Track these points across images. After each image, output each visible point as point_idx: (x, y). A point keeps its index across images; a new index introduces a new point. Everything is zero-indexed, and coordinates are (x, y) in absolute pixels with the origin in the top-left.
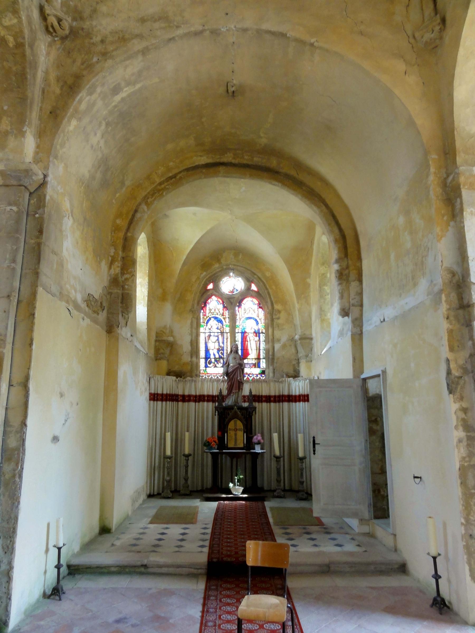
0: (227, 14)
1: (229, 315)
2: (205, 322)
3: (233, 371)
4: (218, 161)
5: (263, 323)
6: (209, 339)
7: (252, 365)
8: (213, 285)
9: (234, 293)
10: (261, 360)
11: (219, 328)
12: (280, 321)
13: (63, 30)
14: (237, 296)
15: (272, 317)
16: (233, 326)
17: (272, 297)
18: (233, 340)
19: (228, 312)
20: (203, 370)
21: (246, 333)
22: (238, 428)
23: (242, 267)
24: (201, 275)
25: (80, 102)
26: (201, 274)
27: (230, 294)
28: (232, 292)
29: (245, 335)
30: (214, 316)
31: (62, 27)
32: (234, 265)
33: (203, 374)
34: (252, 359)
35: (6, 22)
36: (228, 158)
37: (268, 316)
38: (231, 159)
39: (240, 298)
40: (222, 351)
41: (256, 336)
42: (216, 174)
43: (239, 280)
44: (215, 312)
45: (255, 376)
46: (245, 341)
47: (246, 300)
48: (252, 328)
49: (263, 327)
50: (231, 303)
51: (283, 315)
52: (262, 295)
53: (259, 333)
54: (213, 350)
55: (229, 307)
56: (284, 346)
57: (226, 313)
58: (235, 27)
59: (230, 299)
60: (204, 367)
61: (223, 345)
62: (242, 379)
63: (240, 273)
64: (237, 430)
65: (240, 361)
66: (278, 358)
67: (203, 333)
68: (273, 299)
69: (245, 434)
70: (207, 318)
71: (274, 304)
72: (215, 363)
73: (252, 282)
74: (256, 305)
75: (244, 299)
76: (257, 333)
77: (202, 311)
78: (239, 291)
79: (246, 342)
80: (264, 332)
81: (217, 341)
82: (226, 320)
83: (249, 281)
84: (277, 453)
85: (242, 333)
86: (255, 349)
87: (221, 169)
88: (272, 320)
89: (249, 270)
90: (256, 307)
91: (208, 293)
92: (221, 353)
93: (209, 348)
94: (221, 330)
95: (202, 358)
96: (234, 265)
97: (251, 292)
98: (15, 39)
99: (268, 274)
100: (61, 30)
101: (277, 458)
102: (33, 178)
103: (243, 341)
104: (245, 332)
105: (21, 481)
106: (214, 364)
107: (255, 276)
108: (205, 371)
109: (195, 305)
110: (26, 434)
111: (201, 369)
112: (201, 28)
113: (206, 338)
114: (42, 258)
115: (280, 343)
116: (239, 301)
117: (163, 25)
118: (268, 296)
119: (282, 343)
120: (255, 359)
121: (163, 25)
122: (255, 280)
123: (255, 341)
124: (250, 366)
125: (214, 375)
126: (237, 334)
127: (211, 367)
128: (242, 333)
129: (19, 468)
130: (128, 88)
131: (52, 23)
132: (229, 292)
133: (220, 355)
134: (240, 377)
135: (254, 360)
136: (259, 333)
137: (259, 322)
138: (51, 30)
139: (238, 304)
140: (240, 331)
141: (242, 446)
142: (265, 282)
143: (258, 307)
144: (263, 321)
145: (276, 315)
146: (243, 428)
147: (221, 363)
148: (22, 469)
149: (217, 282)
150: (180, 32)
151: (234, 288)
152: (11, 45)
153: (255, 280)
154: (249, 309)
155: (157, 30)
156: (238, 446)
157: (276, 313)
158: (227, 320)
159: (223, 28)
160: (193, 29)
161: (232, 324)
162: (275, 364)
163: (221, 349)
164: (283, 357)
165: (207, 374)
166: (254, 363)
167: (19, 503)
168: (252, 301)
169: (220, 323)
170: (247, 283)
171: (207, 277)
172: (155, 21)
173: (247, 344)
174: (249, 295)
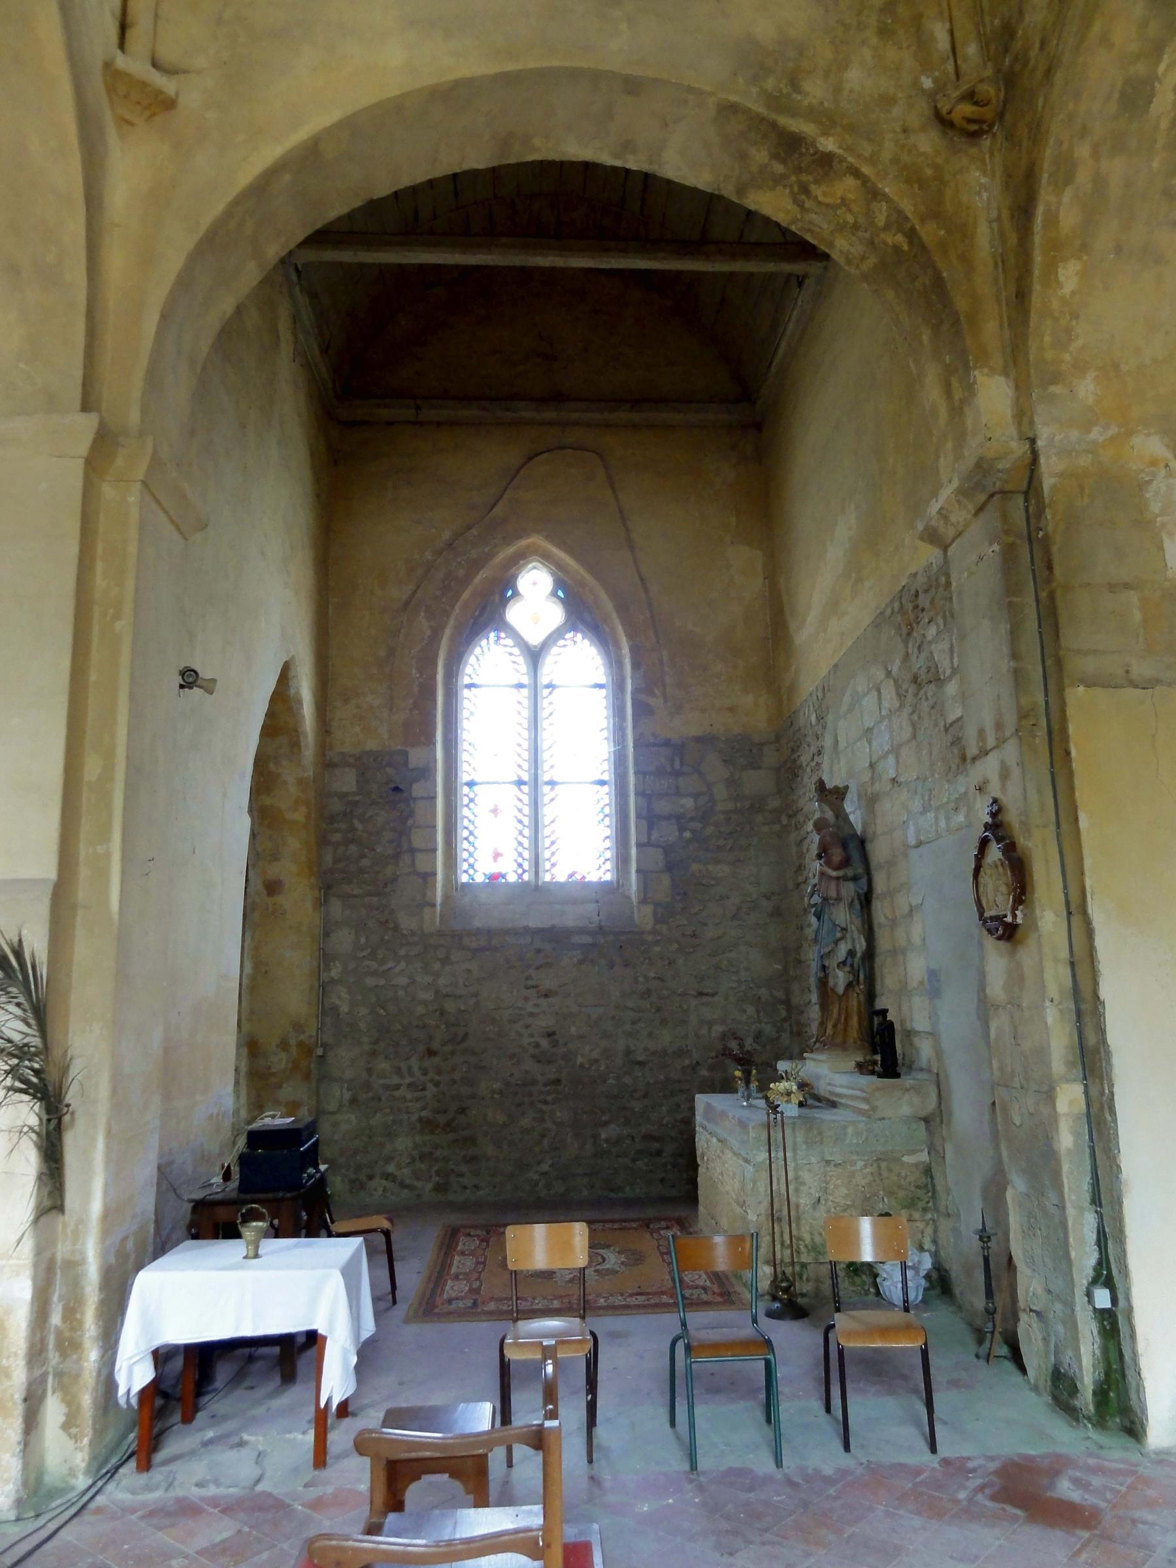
13: (988, 103)
25: (1052, 220)
31: (982, 101)
35: (881, 220)
98: (905, 234)
100: (985, 108)
102: (1000, 466)
105: (1115, 1121)
110: (1105, 1017)
114: (1063, 621)
129: (1107, 1091)
130: (1165, 56)
131: (964, 118)
138: (974, 127)
148: (1112, 1094)
152: (906, 247)
167: (1119, 1167)
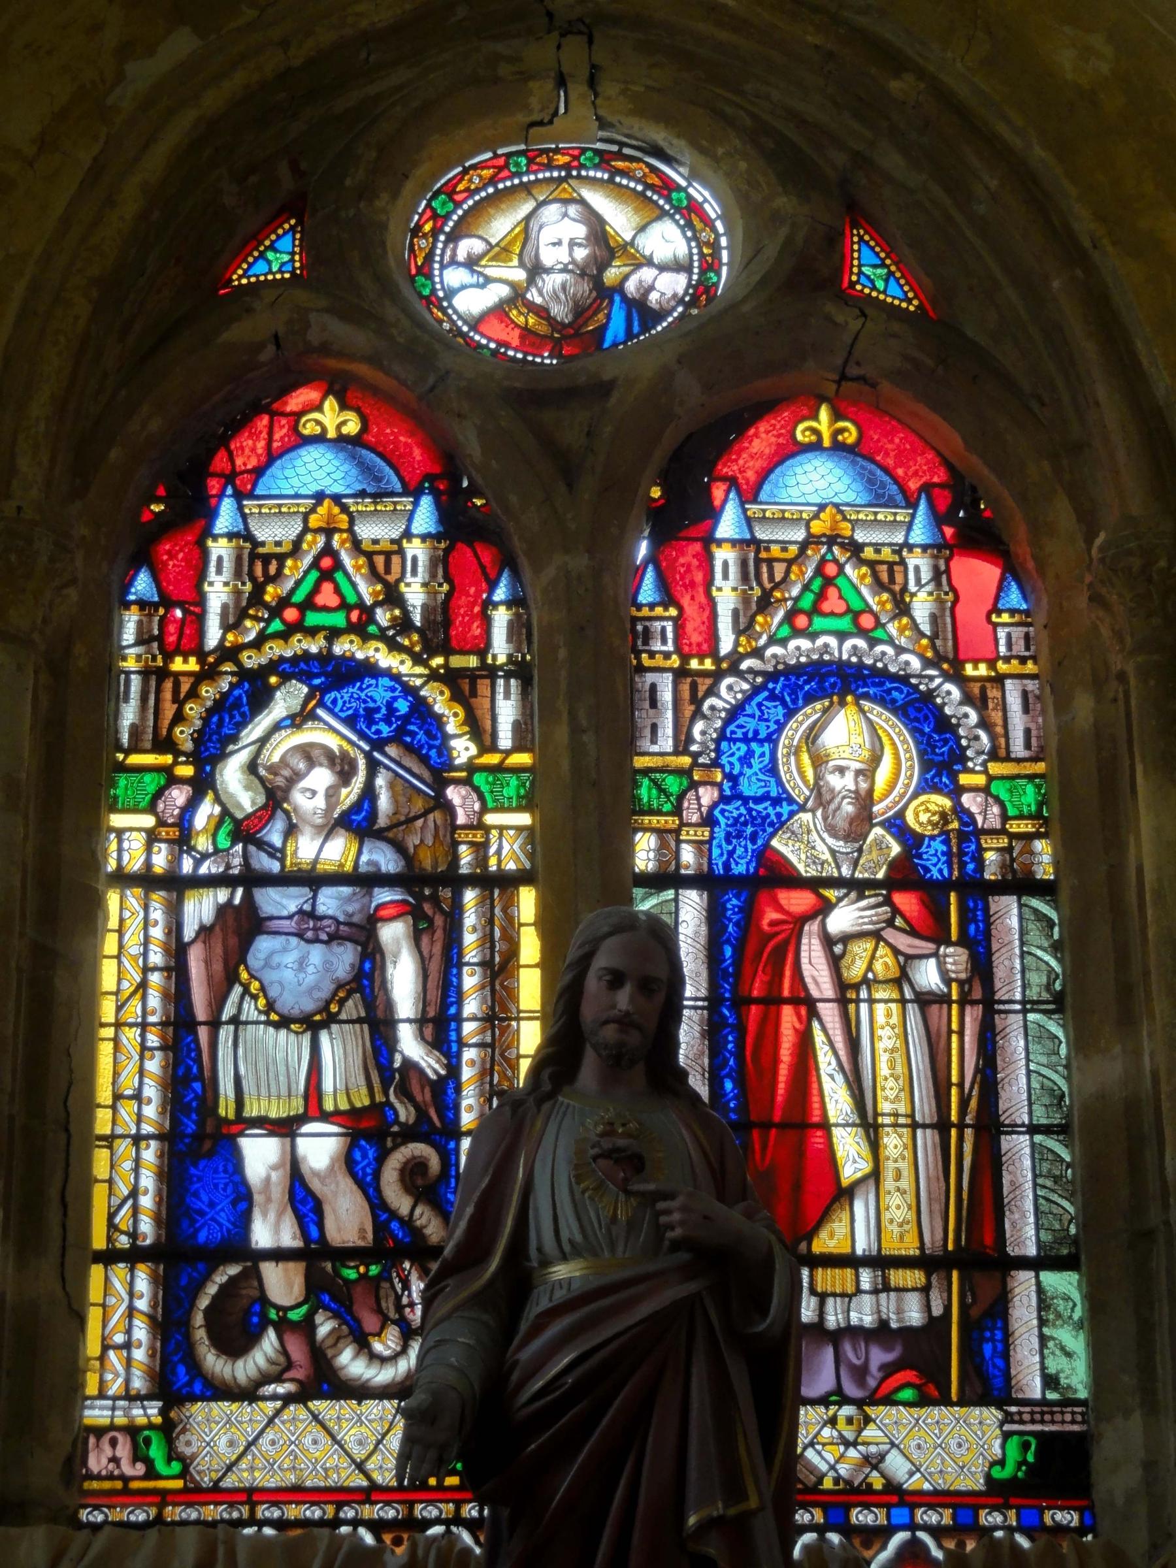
1: (519, 630)
2: (184, 735)
5: (1018, 748)
6: (232, 978)
7: (879, 1357)
8: (309, 247)
10: (1023, 1284)
11: (382, 822)
20: (132, 1430)
21: (789, 879)
24: (131, 68)
26: (126, 51)
30: (301, 644)
33: (126, 1494)
34: (881, 1262)
40: (419, 1149)
44: (327, 596)
45: (937, 1532)
46: (773, 1001)
49: (1029, 796)
54: (285, 1128)
60: (138, 1383)
61: (430, 1063)
62: (764, 1529)
65: (719, 1208)
67: (147, 880)
70: (208, 674)
72: (307, 1327)
77: (143, 585)
79: (787, 1012)
80: (1045, 869)
81: (353, 1008)
82: (481, 704)
86: (925, 1110)
91: (239, 332)
92: (412, 1173)
93: (227, 1108)
94: (413, 841)
95: (109, 1257)
103: (740, 1003)
106: (298, 1351)
108: (156, 1452)
109: (24, 464)
111: (96, 1414)
113: (177, 951)
116: (677, 456)
118: (1088, 349)
120: (923, 1262)
122: (892, 161)
123: (925, 1000)
124: (860, 1374)
125: (293, 1512)
127: (248, 1394)
133: (401, 1202)
134: (734, 1491)
135: (913, 1277)
139: (656, 492)
143: (949, 531)
147: (407, 1333)
149: (366, 193)
153: (892, 161)
154: (814, 556)
163: (405, 1113)
165: (194, 1494)
166: (915, 1316)
169: (392, 750)
170: (782, 202)
171: (213, 101)
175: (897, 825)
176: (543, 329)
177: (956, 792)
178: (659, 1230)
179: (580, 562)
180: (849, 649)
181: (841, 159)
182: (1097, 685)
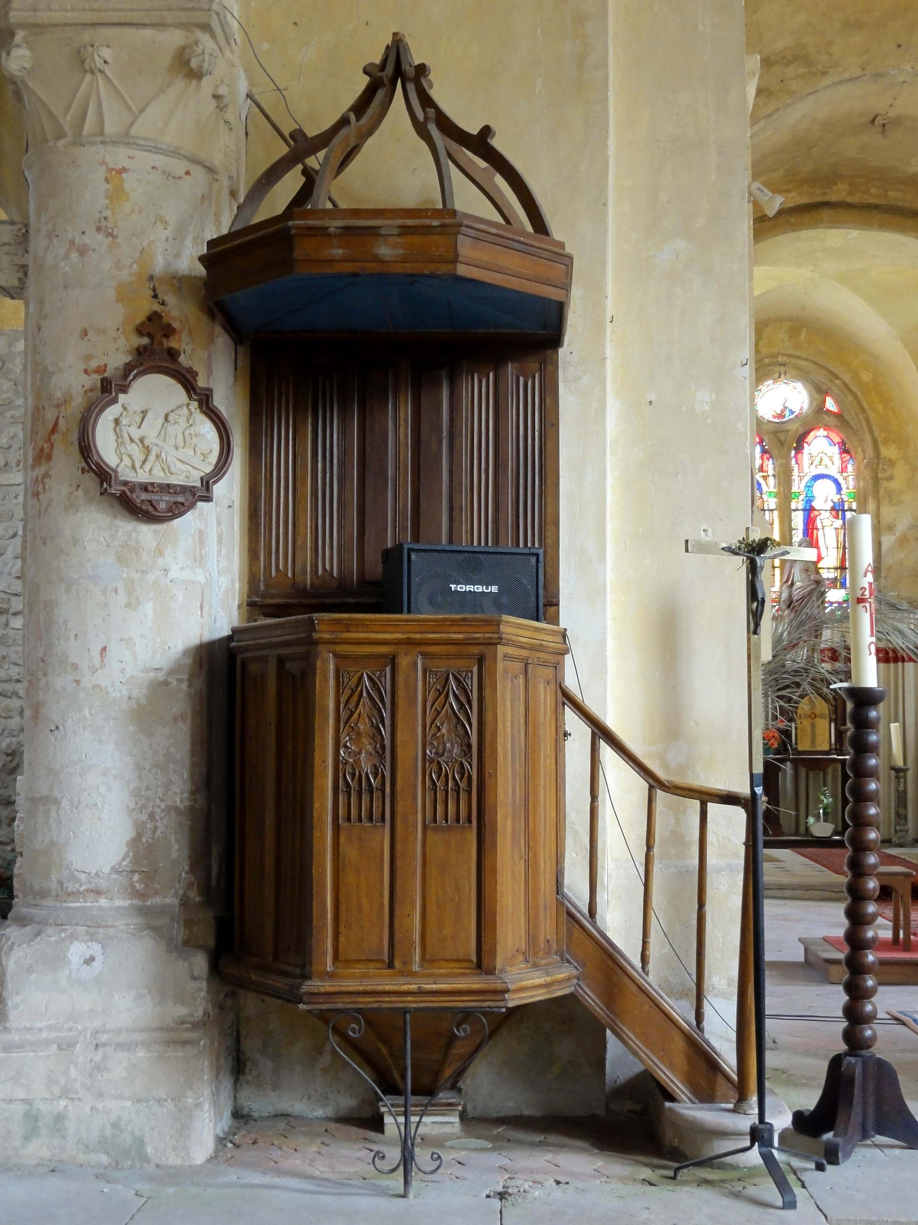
0: (900, 46)
1: (774, 469)
3: (803, 598)
4: (819, 199)
5: (851, 487)
9: (784, 420)
12: (894, 485)
14: (793, 427)
15: (877, 474)
16: (785, 495)
17: (874, 428)
18: (786, 527)
19: (773, 464)
22: (817, 712)
23: (806, 359)
27: (776, 420)
28: (781, 415)
29: (812, 515)
32: (789, 356)
34: (828, 568)
36: (838, 193)
37: (866, 472)
38: (844, 195)
39: (801, 430)
41: (837, 517)
42: (815, 224)
43: (796, 388)
46: (813, 529)
47: (812, 435)
48: (827, 500)
49: (852, 496)
50: (782, 443)
51: (900, 470)
52: (853, 424)
53: (844, 511)
55: (775, 453)
56: (902, 542)
57: (770, 466)
58: (913, 67)
59: (778, 434)
63: (803, 375)
64: (815, 716)
66: (890, 568)
68: (876, 434)
69: (833, 725)
71: (880, 444)
73: (827, 393)
74: (835, 445)
75: (807, 433)
76: (838, 510)
78: (795, 414)
79: (815, 531)
80: (854, 507)
83: (819, 391)
84: (900, 763)
85: (804, 510)
87: (826, 213)
88: (876, 482)
89: (824, 368)
90: (836, 450)
96: (789, 356)
97: (826, 417)
99: (866, 376)
101: (898, 770)
104: (812, 509)
107: (838, 382)
112: (858, 72)
115: (894, 535)
117: (801, 71)
118: (865, 428)
119: (898, 534)
121: (801, 71)
122: (834, 389)
123: (836, 529)
126: (793, 514)
128: (804, 510)
132: (774, 417)
135: (833, 570)
136: (844, 511)
137: (844, 486)
139: (795, 445)
140: (800, 506)
141: (826, 748)
142: (859, 393)
144: (851, 483)
145: (884, 470)
146: (827, 712)
150: (827, 81)
151: (785, 408)
153: (834, 389)
154: (820, 455)
155: (792, 79)
156: (819, 748)
157: (886, 467)
158: (771, 481)
159: (893, 70)
160: (847, 76)
161: (784, 492)
162: (883, 580)
164: (901, 564)
168: (827, 437)
170: (817, 396)
172: (788, 64)
173: (817, 535)
174: (820, 424)
175: (832, 500)
176: (775, 414)
177: (841, 495)
178: (810, 578)
179: (784, 461)
180: (826, 472)
181: (826, 388)
182: (864, 480)
